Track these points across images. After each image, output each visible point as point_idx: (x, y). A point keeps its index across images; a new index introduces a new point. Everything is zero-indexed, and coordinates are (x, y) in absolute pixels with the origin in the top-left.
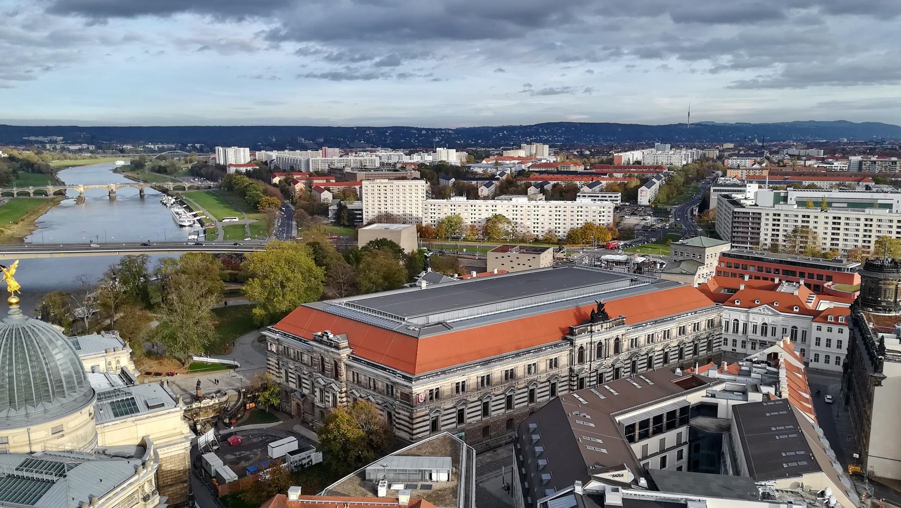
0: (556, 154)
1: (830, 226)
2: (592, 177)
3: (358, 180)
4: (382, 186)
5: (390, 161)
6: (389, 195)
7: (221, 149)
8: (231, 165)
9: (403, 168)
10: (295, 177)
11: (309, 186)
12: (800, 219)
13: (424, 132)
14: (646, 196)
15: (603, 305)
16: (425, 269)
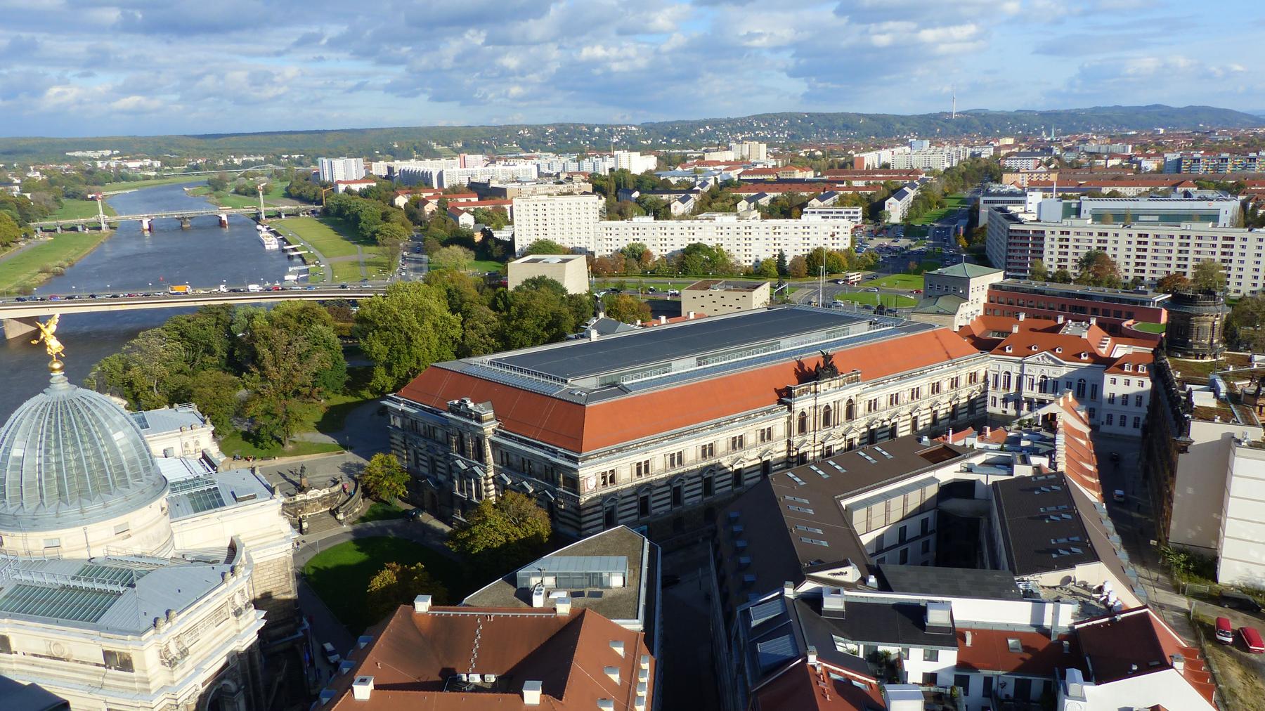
0: (776, 156)
1: (1134, 246)
2: (823, 189)
4: (539, 204)
6: (549, 217)
7: (325, 160)
8: (340, 182)
9: (569, 179)
10: (424, 195)
11: (442, 205)
12: (1095, 237)
13: (597, 130)
14: (895, 211)
15: (831, 357)
16: (595, 315)
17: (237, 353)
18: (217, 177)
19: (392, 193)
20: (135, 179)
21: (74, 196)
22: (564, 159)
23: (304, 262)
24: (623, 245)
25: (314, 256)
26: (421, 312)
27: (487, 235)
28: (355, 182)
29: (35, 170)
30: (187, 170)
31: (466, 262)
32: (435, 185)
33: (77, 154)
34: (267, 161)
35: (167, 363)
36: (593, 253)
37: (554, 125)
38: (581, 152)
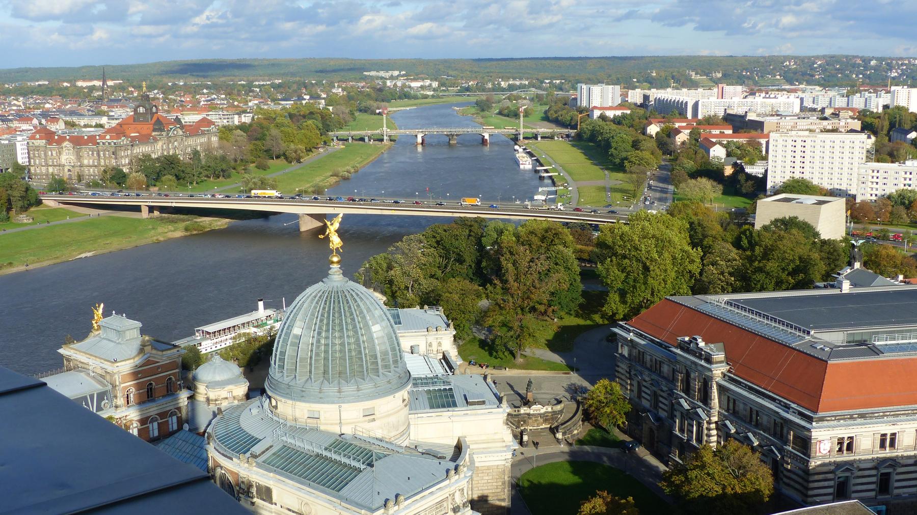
3: (766, 131)
4: (799, 140)
5: (815, 106)
6: (808, 154)
7: (584, 86)
8: (595, 108)
9: (836, 115)
10: (677, 125)
11: (694, 135)
13: (873, 63)
16: (850, 264)
17: (484, 264)
18: (484, 98)
19: (645, 121)
20: (416, 97)
21: (365, 110)
22: (832, 93)
23: (554, 184)
24: (891, 190)
25: (563, 179)
26: (662, 243)
27: (739, 169)
28: (610, 108)
29: (339, 87)
30: (459, 91)
31: (713, 195)
32: (689, 115)
33: (373, 73)
34: (531, 85)
35: (422, 266)
36: (854, 197)
37: (824, 57)
38: (852, 86)
